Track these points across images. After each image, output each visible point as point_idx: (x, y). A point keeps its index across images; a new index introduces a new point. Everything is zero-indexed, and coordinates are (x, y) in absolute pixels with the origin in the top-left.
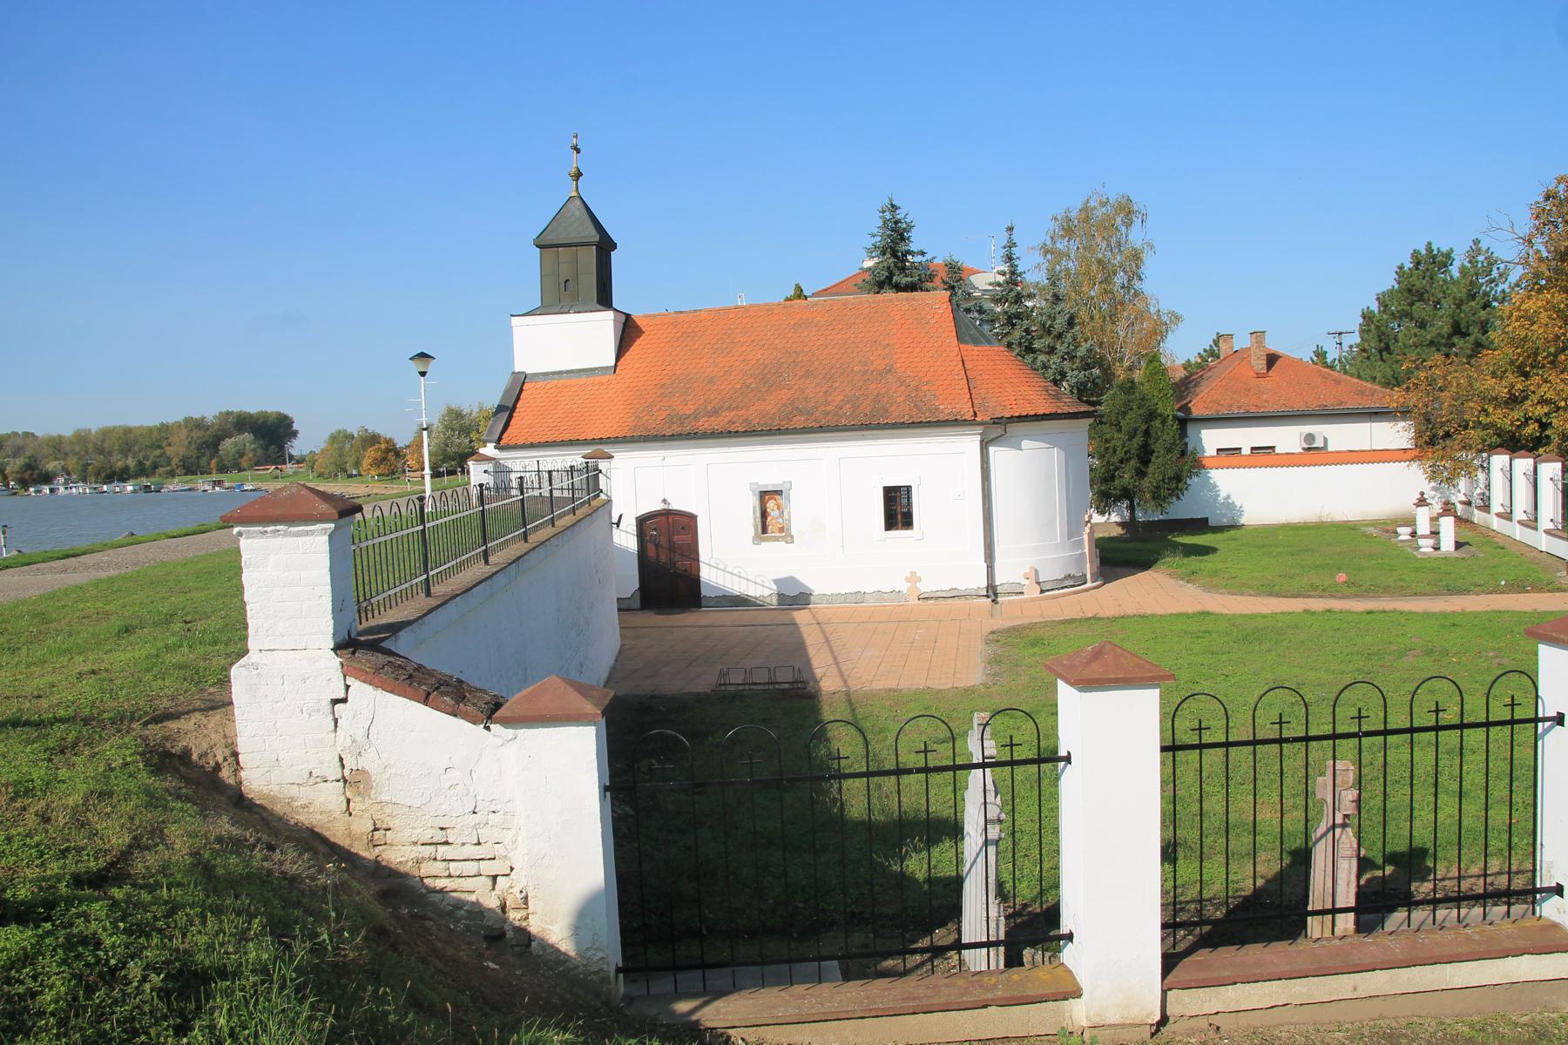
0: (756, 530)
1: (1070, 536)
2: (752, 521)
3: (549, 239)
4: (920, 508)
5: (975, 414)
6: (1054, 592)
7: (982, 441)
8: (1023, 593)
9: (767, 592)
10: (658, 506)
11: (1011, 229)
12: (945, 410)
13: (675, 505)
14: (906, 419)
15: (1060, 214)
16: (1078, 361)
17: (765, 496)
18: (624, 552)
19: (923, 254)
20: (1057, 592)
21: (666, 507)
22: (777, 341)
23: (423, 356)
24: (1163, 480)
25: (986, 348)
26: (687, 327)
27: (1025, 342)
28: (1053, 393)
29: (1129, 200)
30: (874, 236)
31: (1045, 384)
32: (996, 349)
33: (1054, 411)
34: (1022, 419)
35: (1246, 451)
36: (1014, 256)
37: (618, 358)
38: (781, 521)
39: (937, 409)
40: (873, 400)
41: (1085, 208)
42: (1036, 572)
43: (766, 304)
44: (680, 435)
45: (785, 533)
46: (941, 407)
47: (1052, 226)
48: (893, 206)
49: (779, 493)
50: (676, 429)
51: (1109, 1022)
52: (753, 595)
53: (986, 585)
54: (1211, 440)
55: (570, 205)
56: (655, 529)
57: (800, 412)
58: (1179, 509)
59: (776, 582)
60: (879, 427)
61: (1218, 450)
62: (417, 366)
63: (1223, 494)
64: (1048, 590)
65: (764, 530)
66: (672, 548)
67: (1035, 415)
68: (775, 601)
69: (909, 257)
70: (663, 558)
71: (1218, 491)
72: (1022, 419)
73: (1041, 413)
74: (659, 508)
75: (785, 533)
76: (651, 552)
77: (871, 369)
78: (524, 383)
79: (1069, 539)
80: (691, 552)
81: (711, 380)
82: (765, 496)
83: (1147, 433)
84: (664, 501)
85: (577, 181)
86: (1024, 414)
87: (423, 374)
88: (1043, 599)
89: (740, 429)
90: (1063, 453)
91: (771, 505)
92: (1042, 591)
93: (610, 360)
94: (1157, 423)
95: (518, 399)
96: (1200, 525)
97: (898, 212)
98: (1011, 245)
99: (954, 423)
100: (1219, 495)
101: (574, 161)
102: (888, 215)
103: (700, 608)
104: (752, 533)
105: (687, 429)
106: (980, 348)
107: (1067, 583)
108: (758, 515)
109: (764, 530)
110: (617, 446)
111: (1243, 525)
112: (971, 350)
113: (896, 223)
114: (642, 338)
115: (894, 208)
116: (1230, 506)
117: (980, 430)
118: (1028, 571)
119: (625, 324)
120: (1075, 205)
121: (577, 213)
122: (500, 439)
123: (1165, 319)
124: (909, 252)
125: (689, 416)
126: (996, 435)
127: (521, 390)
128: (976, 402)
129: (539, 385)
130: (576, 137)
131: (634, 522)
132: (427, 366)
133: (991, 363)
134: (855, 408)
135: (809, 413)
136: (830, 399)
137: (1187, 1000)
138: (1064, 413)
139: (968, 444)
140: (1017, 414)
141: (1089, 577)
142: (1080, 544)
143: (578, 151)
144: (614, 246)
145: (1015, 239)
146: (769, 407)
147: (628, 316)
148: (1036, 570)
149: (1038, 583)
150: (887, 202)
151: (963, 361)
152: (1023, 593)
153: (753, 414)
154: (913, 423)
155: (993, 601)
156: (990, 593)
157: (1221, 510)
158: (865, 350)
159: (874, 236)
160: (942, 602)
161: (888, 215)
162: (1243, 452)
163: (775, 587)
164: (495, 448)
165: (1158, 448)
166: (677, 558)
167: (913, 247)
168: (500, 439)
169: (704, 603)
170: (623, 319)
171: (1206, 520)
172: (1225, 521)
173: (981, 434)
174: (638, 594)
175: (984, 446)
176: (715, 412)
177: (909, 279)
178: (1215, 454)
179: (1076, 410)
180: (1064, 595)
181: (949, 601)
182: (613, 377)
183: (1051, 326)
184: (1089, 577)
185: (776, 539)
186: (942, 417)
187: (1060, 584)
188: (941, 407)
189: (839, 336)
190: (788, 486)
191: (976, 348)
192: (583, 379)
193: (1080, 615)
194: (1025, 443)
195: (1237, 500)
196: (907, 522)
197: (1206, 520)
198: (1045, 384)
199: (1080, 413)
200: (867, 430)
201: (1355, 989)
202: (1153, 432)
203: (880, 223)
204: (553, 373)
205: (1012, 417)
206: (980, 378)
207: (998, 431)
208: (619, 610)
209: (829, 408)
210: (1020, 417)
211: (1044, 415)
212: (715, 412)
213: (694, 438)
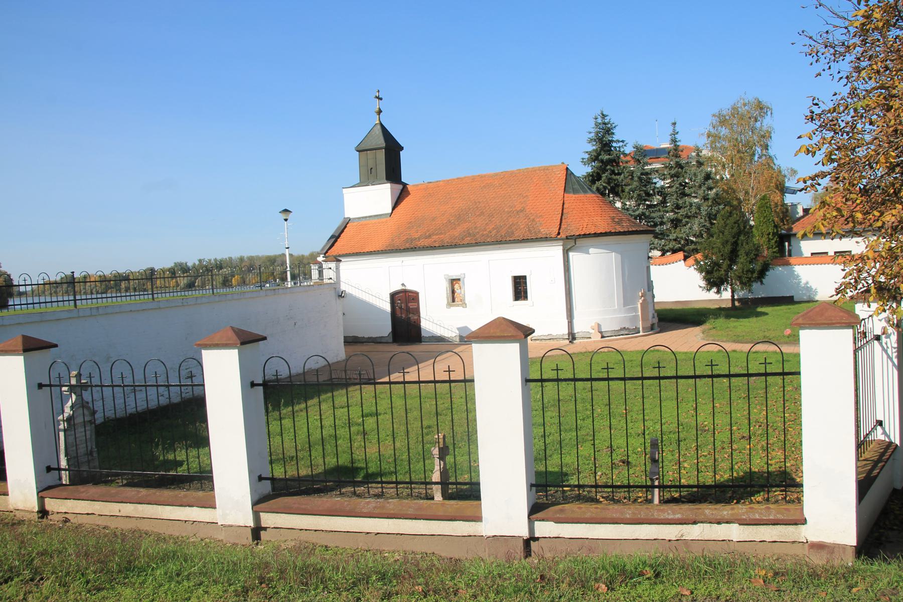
0: (448, 300)
1: (625, 304)
2: (446, 295)
3: (363, 147)
4: (532, 287)
5: (559, 234)
6: (612, 338)
7: (563, 250)
8: (590, 338)
9: (454, 335)
10: (399, 287)
11: (674, 124)
12: (544, 231)
13: (409, 287)
14: (521, 238)
15: (716, 111)
16: (710, 201)
17: (454, 282)
18: (383, 311)
19: (623, 141)
20: (614, 337)
21: (404, 288)
22: (471, 196)
23: (286, 211)
24: (743, 272)
25: (580, 195)
26: (432, 190)
27: (679, 191)
28: (617, 220)
29: (760, 102)
30: (590, 133)
31: (615, 215)
32: (588, 196)
33: (609, 231)
34: (585, 236)
35: (831, 253)
36: (677, 140)
37: (393, 209)
38: (461, 295)
39: (539, 231)
40: (509, 228)
41: (735, 109)
42: (599, 326)
43: (473, 176)
44: (408, 249)
45: (464, 304)
46: (542, 230)
47: (715, 121)
48: (603, 115)
49: (459, 280)
50: (407, 246)
51: (20, 508)
52: (447, 336)
53: (567, 332)
54: (808, 247)
55: (375, 128)
56: (399, 300)
57: (469, 234)
58: (759, 291)
59: (458, 329)
60: (506, 242)
61: (812, 254)
62: (283, 216)
63: (803, 281)
64: (608, 337)
65: (453, 301)
66: (408, 310)
67: (595, 233)
68: (458, 340)
69: (614, 144)
70: (404, 316)
71: (800, 279)
72: (585, 236)
73: (599, 232)
74: (400, 289)
75: (464, 304)
76: (399, 314)
77: (514, 209)
78: (348, 223)
79: (624, 307)
80: (417, 311)
81: (434, 219)
82: (454, 282)
83: (735, 244)
84: (403, 285)
85: (379, 115)
86: (588, 233)
87: (286, 220)
88: (601, 341)
89: (437, 245)
90: (619, 256)
91: (456, 286)
92: (603, 337)
93: (390, 211)
94: (742, 237)
95: (342, 231)
96: (789, 300)
97: (606, 118)
98: (675, 133)
99: (545, 239)
100: (801, 282)
101: (377, 104)
102: (599, 120)
103: (421, 342)
104: (446, 302)
105: (412, 246)
106: (577, 196)
107: (622, 332)
108: (450, 292)
109: (453, 301)
110: (379, 255)
111: (817, 301)
112: (570, 197)
113: (605, 124)
114: (410, 196)
115: (604, 116)
116: (809, 289)
117: (561, 243)
118: (593, 324)
119: (402, 190)
120: (725, 105)
121: (377, 133)
122: (327, 252)
123: (784, 172)
124: (612, 141)
125: (416, 239)
126: (571, 246)
127: (345, 227)
128: (563, 226)
129: (355, 224)
130: (379, 91)
131: (389, 296)
132: (288, 216)
133: (581, 204)
134: (498, 232)
135: (474, 236)
136: (487, 227)
137: (53, 504)
138: (615, 232)
139: (555, 251)
140: (583, 233)
141: (641, 329)
142: (635, 309)
143: (381, 99)
144: (402, 148)
145: (677, 130)
146: (457, 232)
147: (405, 185)
148: (598, 324)
149: (601, 332)
150: (599, 113)
151: (563, 204)
152: (590, 338)
153: (446, 238)
154: (523, 239)
155: (570, 342)
156: (570, 337)
157: (802, 291)
158: (514, 199)
159: (590, 133)
160: (544, 342)
161: (599, 120)
162: (829, 254)
163: (458, 332)
164: (323, 257)
165: (742, 252)
166: (411, 315)
167: (615, 138)
168: (327, 252)
169: (423, 340)
170: (401, 187)
171: (792, 297)
172: (805, 298)
173: (563, 245)
174: (391, 334)
175: (566, 253)
176: (430, 236)
177: (608, 157)
178: (810, 255)
179: (626, 230)
180: (617, 340)
181: (548, 342)
182: (390, 218)
183: (695, 181)
184: (641, 329)
185: (458, 305)
186: (540, 236)
187: (617, 333)
188: (542, 230)
189: (503, 192)
190: (463, 276)
191: (574, 196)
192: (376, 220)
193: (584, 350)
194: (591, 250)
195: (813, 285)
196: (526, 298)
197: (792, 297)
198: (615, 215)
199: (628, 231)
200: (499, 244)
201: (120, 511)
202: (740, 242)
203: (594, 126)
204: (363, 218)
205: (580, 235)
206: (571, 213)
207: (571, 243)
208: (344, 342)
209: (484, 233)
210: (584, 235)
211: (601, 233)
212: (430, 236)
213: (414, 251)
